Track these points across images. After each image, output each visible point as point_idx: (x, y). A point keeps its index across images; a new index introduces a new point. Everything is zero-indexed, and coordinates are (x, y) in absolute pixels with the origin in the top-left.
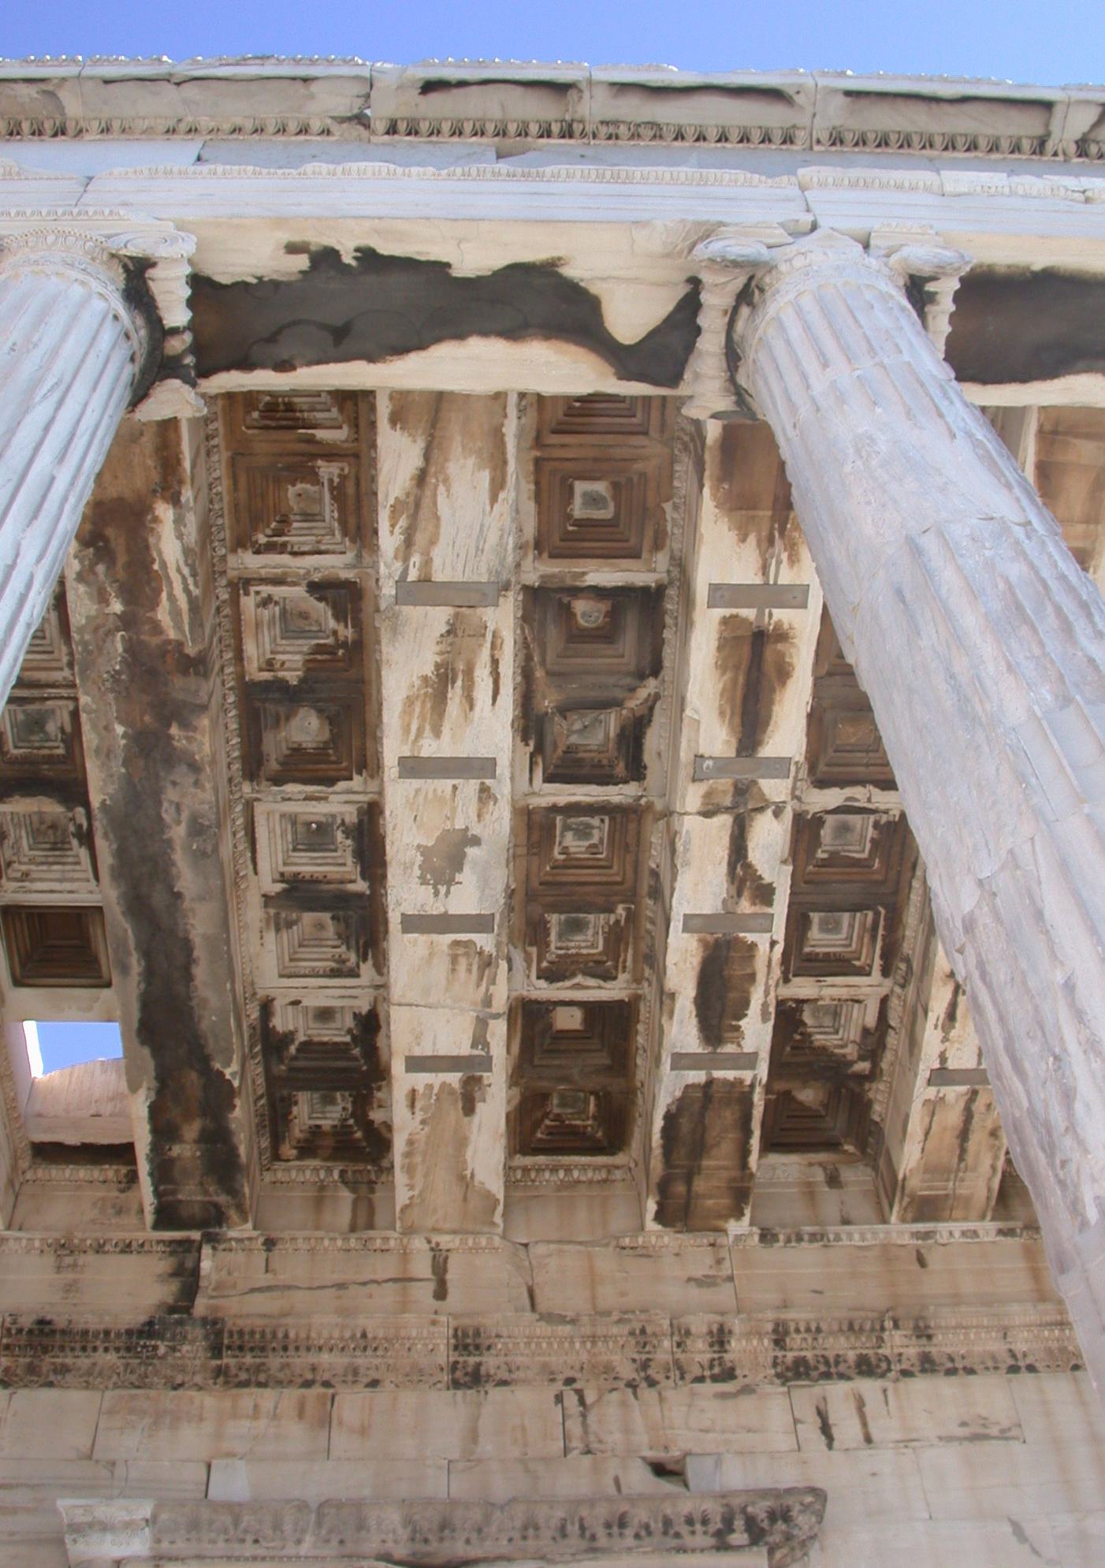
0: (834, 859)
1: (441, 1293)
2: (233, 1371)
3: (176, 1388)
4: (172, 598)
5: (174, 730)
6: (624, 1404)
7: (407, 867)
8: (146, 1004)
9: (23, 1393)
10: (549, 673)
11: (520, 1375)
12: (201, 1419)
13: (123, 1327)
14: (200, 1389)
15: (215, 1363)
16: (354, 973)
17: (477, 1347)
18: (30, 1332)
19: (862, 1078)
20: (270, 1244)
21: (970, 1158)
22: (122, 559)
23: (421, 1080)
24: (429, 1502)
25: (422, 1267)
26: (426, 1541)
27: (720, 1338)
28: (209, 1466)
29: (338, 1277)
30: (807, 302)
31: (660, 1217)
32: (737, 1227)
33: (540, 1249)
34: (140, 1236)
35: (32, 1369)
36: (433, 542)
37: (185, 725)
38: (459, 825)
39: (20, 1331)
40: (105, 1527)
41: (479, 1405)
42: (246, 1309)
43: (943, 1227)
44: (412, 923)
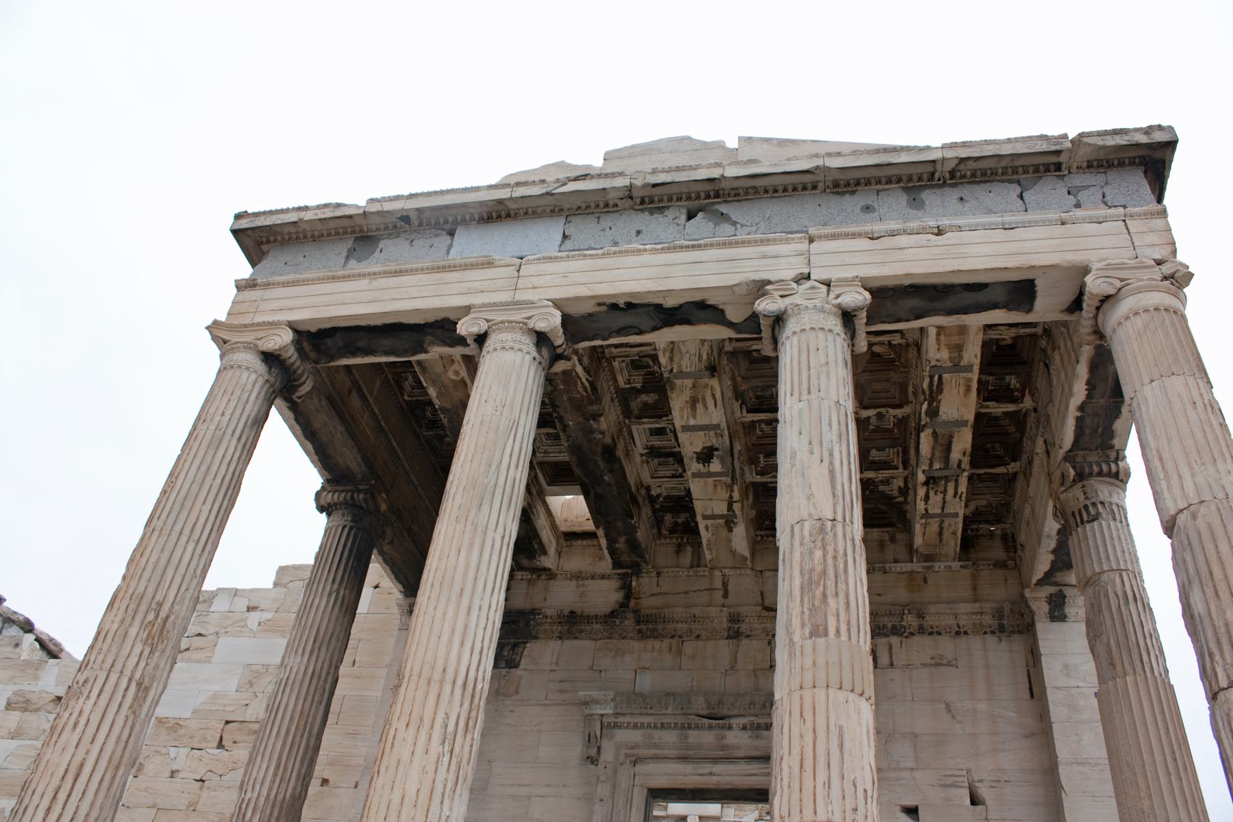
0: (878, 430)
1: (726, 596)
7: (691, 458)
9: (567, 642)
10: (743, 378)
14: (632, 638)
19: (900, 503)
20: (659, 574)
23: (709, 522)
25: (718, 584)
34: (609, 572)
35: (569, 631)
37: (594, 420)
38: (709, 444)
40: (597, 702)
42: (648, 603)
43: (936, 565)
44: (695, 475)
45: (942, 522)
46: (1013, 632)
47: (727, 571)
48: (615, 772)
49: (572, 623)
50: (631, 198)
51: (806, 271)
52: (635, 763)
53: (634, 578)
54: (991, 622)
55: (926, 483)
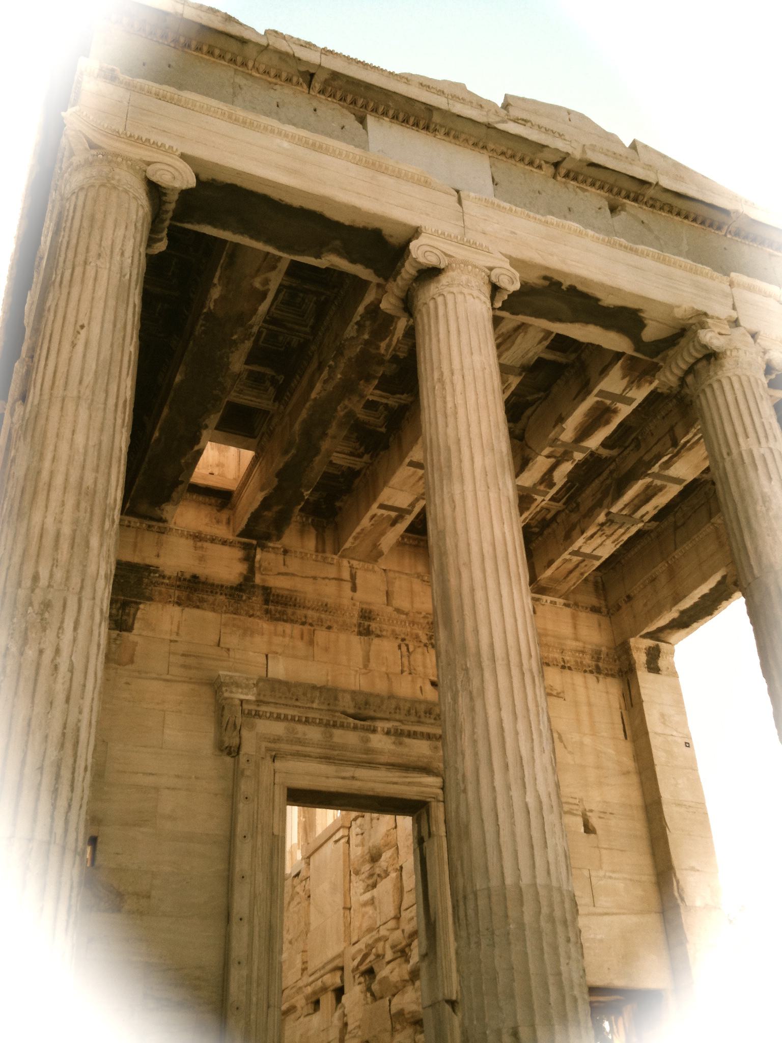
1: (354, 589)
2: (273, 612)
3: (251, 616)
4: (391, 340)
5: (362, 382)
6: (423, 654)
9: (187, 609)
11: (384, 633)
12: (263, 634)
13: (229, 584)
14: (260, 618)
15: (266, 607)
16: (360, 456)
17: (369, 618)
18: (189, 581)
19: (534, 533)
21: (568, 579)
24: (361, 693)
25: (346, 575)
26: (360, 708)
28: (267, 656)
29: (313, 573)
35: (189, 598)
36: (507, 350)
39: (185, 580)
40: (238, 685)
41: (370, 645)
42: (278, 583)
43: (544, 598)
44: (412, 464)
45: (584, 561)
46: (607, 675)
48: (258, 766)
49: (193, 589)
50: (556, 165)
51: (734, 315)
52: (274, 759)
53: (259, 550)
54: (590, 662)
55: (602, 525)
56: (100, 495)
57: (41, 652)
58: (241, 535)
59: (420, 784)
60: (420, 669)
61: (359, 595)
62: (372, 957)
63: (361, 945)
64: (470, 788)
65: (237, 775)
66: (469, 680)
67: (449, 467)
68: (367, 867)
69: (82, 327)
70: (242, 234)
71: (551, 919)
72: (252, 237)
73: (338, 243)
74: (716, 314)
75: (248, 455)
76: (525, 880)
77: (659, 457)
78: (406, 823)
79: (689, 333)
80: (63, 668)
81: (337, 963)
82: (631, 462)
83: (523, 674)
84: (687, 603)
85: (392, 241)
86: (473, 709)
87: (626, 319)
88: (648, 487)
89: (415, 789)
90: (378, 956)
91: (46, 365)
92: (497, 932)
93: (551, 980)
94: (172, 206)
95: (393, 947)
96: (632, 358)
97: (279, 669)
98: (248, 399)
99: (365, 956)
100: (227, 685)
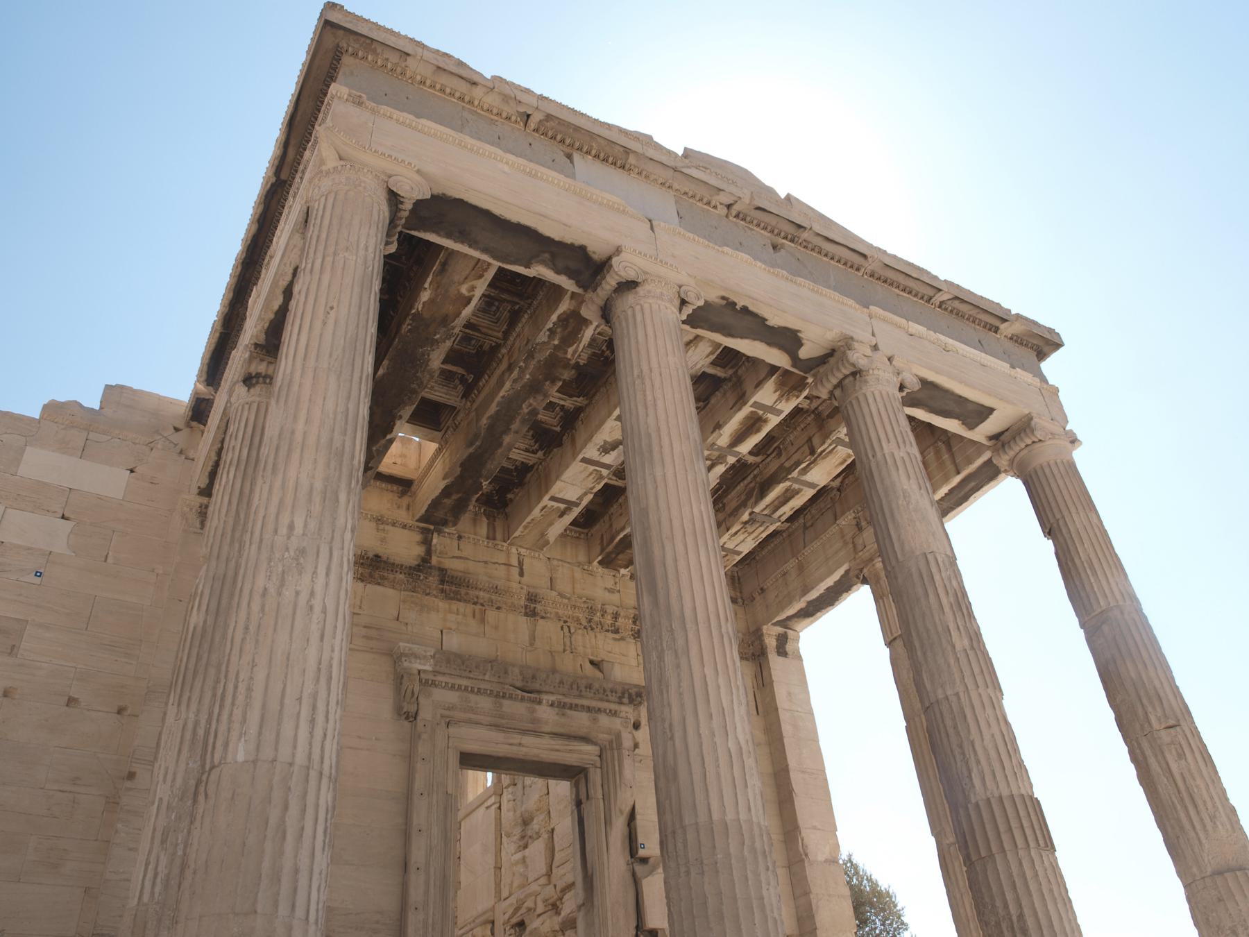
1: (521, 574)
8: (470, 456)
16: (534, 452)
20: (460, 538)
22: (569, 329)
25: (515, 562)
27: (616, 616)
29: (485, 559)
30: (877, 393)
31: (600, 563)
32: (623, 571)
33: (555, 563)
35: (371, 576)
40: (416, 656)
42: (453, 565)
44: (584, 460)
47: (523, 551)
53: (435, 535)
55: (746, 523)
56: (347, 457)
57: (297, 593)
58: (421, 520)
59: (580, 752)
60: (580, 649)
61: (525, 579)
62: (523, 910)
63: (513, 900)
64: (678, 735)
65: (414, 738)
66: (674, 640)
67: (651, 452)
68: (518, 831)
69: (332, 308)
70: (462, 242)
71: (753, 850)
72: (470, 246)
73: (547, 255)
74: (861, 339)
75: (433, 446)
76: (730, 816)
77: (798, 464)
78: (561, 789)
79: (837, 355)
80: (317, 609)
81: (488, 916)
82: (773, 467)
83: (722, 637)
84: (814, 595)
85: (595, 257)
86: (678, 666)
87: (788, 339)
88: (787, 490)
89: (575, 756)
90: (529, 910)
91: (298, 340)
92: (705, 862)
93: (755, 904)
94: (406, 214)
95: (545, 901)
96: (786, 373)
97: (453, 642)
98: (438, 393)
99: (517, 910)
100: (406, 655)
